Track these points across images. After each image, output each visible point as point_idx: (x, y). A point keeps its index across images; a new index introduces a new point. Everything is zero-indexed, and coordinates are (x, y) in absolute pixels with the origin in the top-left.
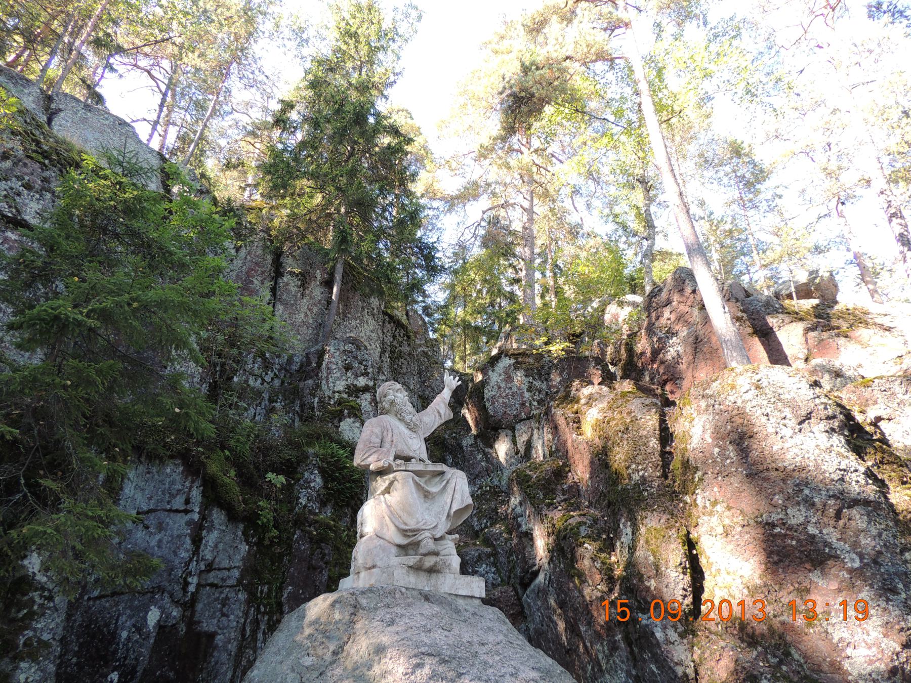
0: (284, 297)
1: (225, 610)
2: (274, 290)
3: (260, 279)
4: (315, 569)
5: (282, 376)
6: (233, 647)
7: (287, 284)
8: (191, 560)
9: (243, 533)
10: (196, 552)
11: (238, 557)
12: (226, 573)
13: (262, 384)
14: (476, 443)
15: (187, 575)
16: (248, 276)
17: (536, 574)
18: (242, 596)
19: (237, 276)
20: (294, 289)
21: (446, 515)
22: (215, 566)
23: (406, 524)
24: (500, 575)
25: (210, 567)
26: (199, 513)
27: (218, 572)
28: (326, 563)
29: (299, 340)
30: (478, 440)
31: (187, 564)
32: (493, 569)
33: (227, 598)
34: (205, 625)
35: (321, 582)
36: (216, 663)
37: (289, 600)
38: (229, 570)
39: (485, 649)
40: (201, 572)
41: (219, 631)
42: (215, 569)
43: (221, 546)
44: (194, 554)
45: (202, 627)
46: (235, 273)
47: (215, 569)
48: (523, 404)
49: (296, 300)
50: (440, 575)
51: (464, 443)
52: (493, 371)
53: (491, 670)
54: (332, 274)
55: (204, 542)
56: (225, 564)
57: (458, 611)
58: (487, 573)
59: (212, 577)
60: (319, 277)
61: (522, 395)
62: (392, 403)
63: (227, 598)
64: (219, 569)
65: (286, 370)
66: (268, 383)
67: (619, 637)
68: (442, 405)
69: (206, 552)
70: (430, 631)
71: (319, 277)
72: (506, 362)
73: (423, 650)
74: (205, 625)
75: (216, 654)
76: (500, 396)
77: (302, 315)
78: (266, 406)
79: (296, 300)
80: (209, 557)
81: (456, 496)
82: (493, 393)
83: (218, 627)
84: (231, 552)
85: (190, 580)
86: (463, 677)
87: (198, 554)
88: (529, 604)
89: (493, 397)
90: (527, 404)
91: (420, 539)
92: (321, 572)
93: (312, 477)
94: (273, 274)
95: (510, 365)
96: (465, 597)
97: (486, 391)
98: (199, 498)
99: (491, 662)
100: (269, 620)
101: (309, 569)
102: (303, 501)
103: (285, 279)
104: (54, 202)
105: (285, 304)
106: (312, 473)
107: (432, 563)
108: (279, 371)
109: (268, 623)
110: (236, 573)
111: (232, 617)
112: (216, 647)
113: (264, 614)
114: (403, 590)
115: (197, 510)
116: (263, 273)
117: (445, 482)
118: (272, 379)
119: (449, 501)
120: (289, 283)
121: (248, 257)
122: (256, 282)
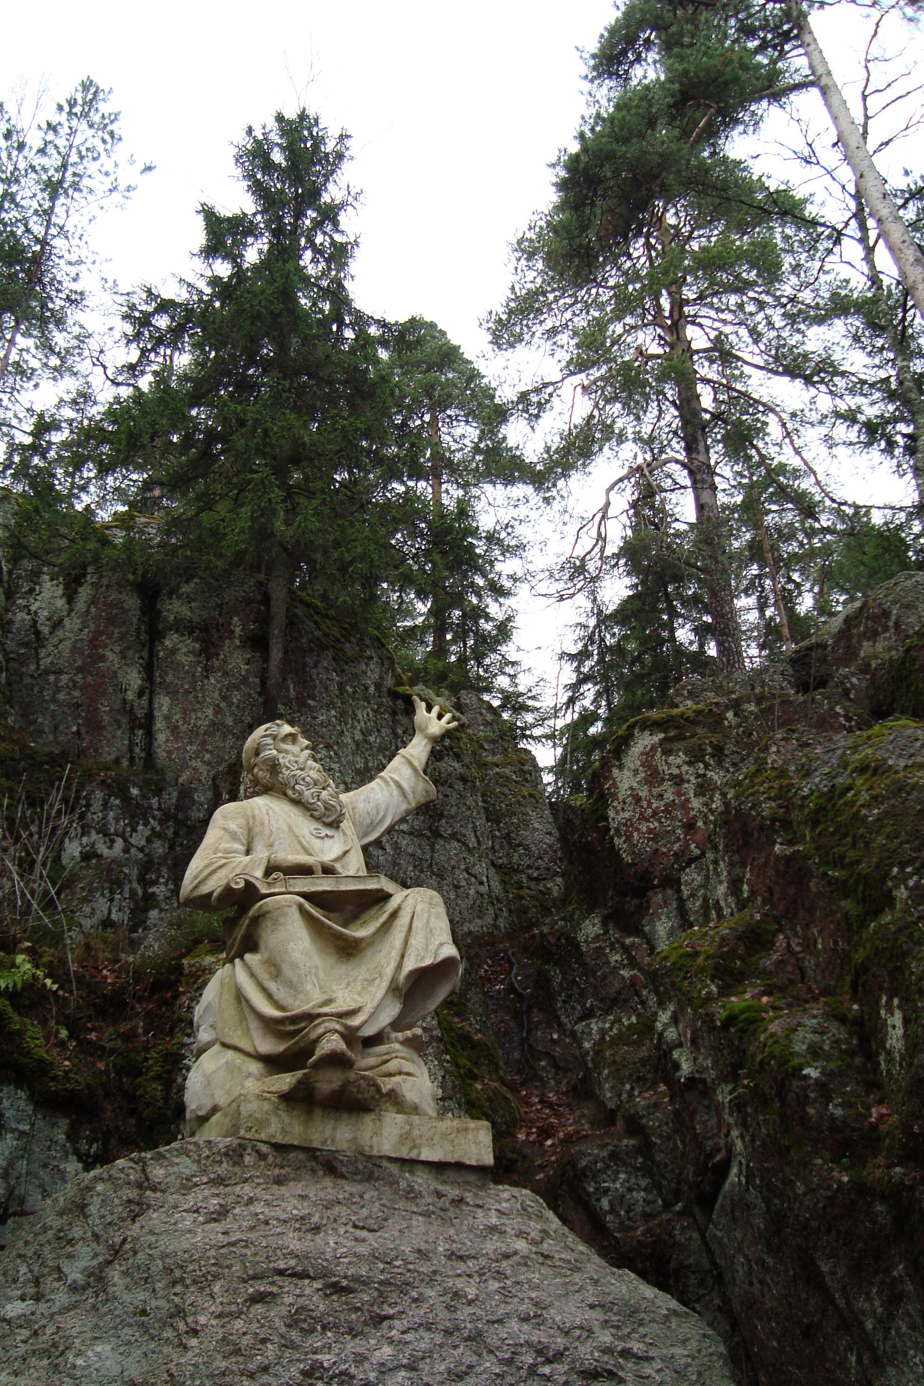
0: (169, 679)
2: (149, 670)
3: (117, 649)
5: (170, 832)
7: (173, 651)
13: (126, 851)
14: (606, 932)
16: (95, 647)
17: (723, 1169)
19: (74, 649)
20: (185, 659)
21: (385, 985)
23: (282, 1008)
24: (660, 1193)
29: (208, 763)
30: (611, 925)
32: (644, 1183)
39: (461, 1267)
46: (68, 643)
47: (15, 1214)
48: (690, 826)
49: (193, 683)
50: (368, 1119)
51: (581, 937)
52: (621, 767)
53: (471, 1310)
54: (265, 620)
57: (411, 1194)
58: (630, 1190)
60: (238, 630)
61: (685, 806)
62: (274, 767)
65: (178, 823)
66: (141, 850)
67: (899, 1269)
68: (407, 772)
70: (316, 1229)
71: (238, 630)
72: (644, 741)
73: (282, 1265)
76: (643, 818)
77: (210, 712)
78: (133, 893)
79: (193, 683)
81: (413, 941)
82: (627, 815)
84: (47, 1178)
86: (386, 1324)
88: (719, 1241)
89: (628, 823)
90: (700, 824)
91: (314, 1035)
94: (143, 637)
95: (653, 748)
96: (439, 1167)
97: (611, 814)
99: (471, 1292)
103: (167, 643)
105: (173, 693)
107: (336, 1084)
108: (161, 822)
114: (264, 1149)
116: (123, 636)
117: (385, 916)
118: (149, 840)
119: (395, 954)
120: (180, 648)
121: (93, 610)
122: (110, 656)
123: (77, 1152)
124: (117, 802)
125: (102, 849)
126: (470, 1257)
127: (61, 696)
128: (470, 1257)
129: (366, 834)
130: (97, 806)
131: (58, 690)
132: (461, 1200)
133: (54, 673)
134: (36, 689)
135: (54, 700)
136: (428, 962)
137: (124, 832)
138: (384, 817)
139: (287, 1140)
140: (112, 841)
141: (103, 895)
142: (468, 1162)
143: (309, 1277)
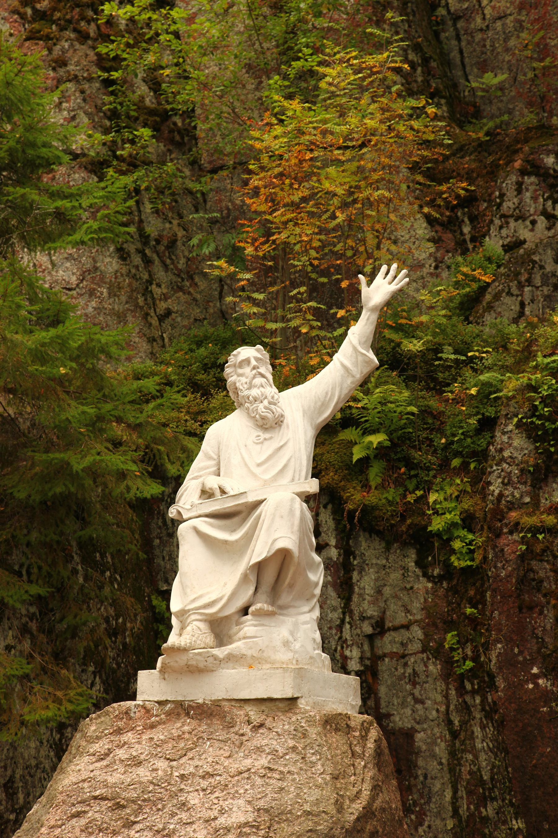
1: (417, 692)
4: (531, 608)
6: (441, 749)
8: (343, 621)
9: (417, 563)
10: (347, 609)
11: (416, 605)
12: (404, 635)
15: (342, 647)
18: (434, 668)
22: (388, 624)
25: (381, 627)
26: (336, 547)
27: (392, 633)
28: (545, 596)
31: (340, 628)
33: (415, 673)
34: (397, 719)
35: (544, 630)
36: (426, 777)
37: (500, 668)
38: (407, 627)
39: (204, 784)
40: (371, 638)
41: (417, 727)
42: (389, 629)
43: (387, 591)
44: (344, 613)
45: (394, 722)
47: (389, 629)
55: (356, 589)
56: (401, 618)
59: (388, 643)
63: (415, 673)
64: (396, 629)
69: (365, 605)
70: (139, 764)
73: (97, 793)
74: (397, 719)
75: (420, 762)
78: (545, 279)
80: (372, 611)
83: (415, 719)
85: (347, 653)
87: (351, 612)
92: (541, 613)
93: (505, 438)
98: (331, 524)
100: (482, 701)
101: (520, 609)
102: (495, 488)
104: (82, 92)
106: (504, 433)
109: (483, 709)
110: (417, 632)
111: (429, 703)
112: (418, 753)
113: (474, 692)
115: (333, 542)
123: (425, 575)
124: (533, 179)
125: (525, 234)
126: (216, 775)
127: (512, 43)
128: (216, 775)
129: (320, 413)
130: (511, 193)
131: (506, 40)
132: (261, 725)
133: (500, 18)
134: (488, 43)
135: (507, 50)
136: (263, 556)
137: (545, 209)
138: (333, 395)
139: (163, 698)
140: (533, 223)
141: (510, 294)
142: (275, 696)
143: (108, 799)
